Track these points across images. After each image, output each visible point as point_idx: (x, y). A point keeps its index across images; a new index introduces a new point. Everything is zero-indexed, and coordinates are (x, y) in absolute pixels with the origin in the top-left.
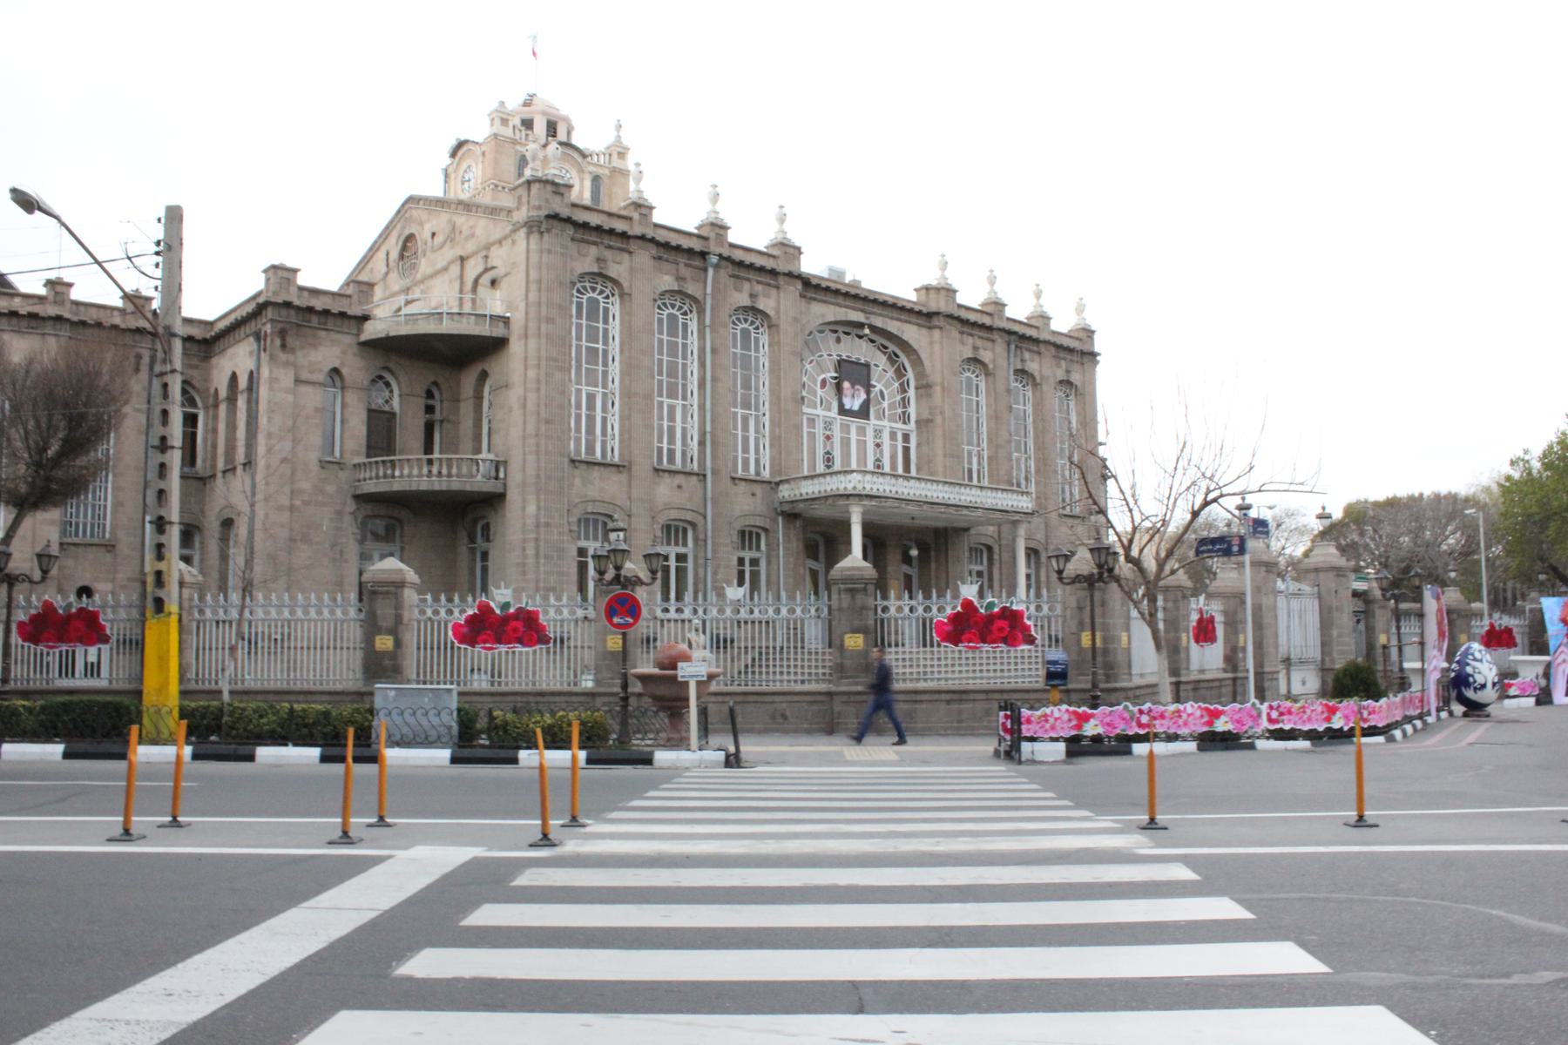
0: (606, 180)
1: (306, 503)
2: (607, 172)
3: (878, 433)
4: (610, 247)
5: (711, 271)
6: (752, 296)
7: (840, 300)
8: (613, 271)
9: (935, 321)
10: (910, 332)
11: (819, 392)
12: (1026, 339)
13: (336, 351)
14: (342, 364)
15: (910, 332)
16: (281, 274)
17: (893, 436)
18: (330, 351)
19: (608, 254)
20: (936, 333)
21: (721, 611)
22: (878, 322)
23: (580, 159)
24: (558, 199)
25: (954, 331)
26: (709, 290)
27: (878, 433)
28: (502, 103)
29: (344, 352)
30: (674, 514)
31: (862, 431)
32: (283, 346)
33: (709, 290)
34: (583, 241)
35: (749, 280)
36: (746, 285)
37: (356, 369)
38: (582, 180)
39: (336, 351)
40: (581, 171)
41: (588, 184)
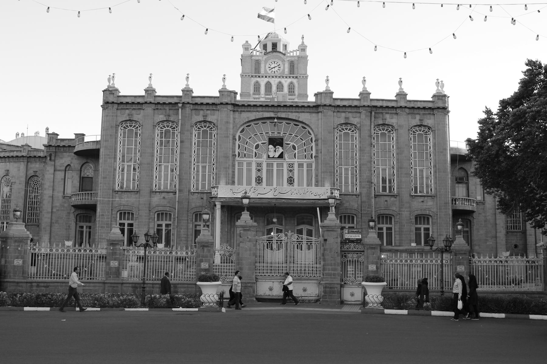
0: (296, 63)
1: (58, 210)
2: (296, 58)
3: (291, 165)
4: (134, 109)
5: (180, 110)
6: (203, 116)
7: (260, 109)
8: (135, 118)
9: (320, 109)
10: (304, 117)
11: (254, 150)
12: (402, 106)
13: (69, 158)
14: (71, 163)
15: (304, 117)
16: (53, 136)
17: (301, 165)
18: (66, 159)
19: (134, 112)
20: (320, 114)
21: (63, 250)
22: (283, 115)
23: (282, 56)
24: (112, 96)
25: (329, 112)
26: (180, 118)
27: (291, 165)
28: (247, 42)
29: (72, 159)
30: (160, 208)
31: (280, 165)
32: (50, 159)
33: (180, 118)
34: (122, 109)
35: (202, 110)
36: (201, 112)
37: (76, 163)
38: (284, 65)
39: (69, 158)
40: (283, 61)
41: (287, 65)
